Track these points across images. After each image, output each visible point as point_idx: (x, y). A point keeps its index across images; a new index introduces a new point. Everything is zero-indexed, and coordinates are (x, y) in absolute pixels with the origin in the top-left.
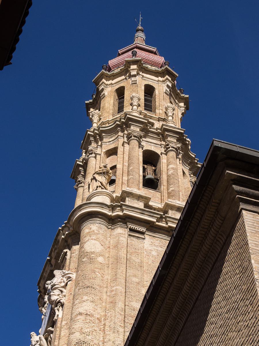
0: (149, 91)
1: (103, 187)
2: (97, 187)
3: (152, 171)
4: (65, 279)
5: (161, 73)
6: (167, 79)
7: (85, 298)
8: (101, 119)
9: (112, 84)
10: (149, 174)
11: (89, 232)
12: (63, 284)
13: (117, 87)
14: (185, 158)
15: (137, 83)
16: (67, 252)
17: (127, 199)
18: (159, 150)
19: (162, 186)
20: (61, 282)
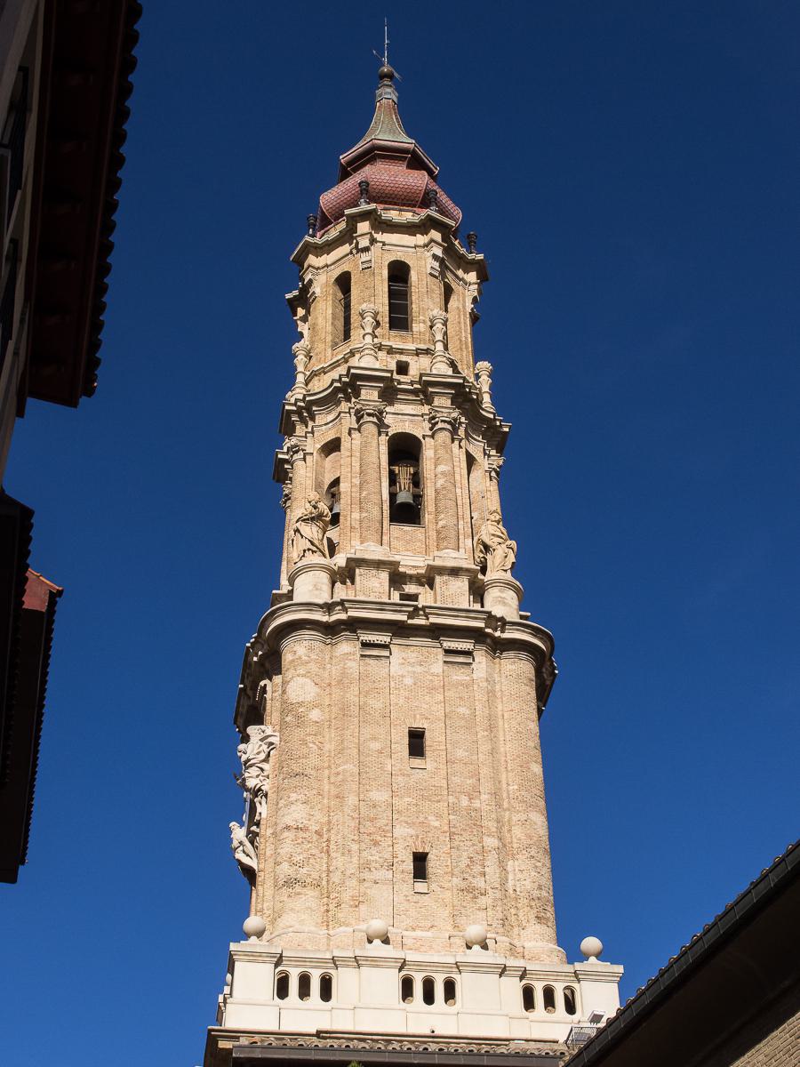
0: (399, 273)
1: (314, 549)
2: (304, 551)
4: (265, 747)
5: (420, 227)
6: (432, 241)
7: (294, 796)
9: (327, 266)
11: (293, 661)
12: (262, 756)
13: (336, 272)
16: (265, 685)
17: (357, 571)
18: (419, 429)
19: (426, 515)
20: (258, 753)
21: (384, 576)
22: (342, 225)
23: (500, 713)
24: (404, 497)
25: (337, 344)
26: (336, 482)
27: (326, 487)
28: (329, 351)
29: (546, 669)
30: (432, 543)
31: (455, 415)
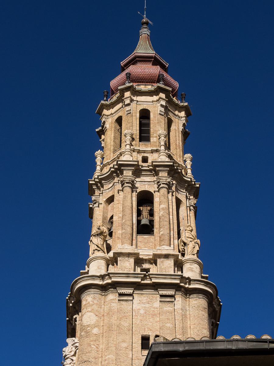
0: (145, 115)
1: (99, 249)
2: (94, 250)
3: (148, 213)
4: (74, 349)
6: (160, 98)
8: (104, 157)
9: (112, 114)
10: (144, 217)
11: (86, 304)
12: (73, 353)
13: (116, 117)
14: (181, 184)
15: (132, 112)
16: (76, 318)
17: (119, 258)
18: (152, 188)
20: (71, 352)
21: (132, 260)
22: (118, 95)
23: (189, 326)
24: (145, 221)
25: (116, 150)
26: (112, 217)
27: (108, 219)
28: (112, 154)
29: (215, 302)
30: (157, 242)
31: (169, 180)
